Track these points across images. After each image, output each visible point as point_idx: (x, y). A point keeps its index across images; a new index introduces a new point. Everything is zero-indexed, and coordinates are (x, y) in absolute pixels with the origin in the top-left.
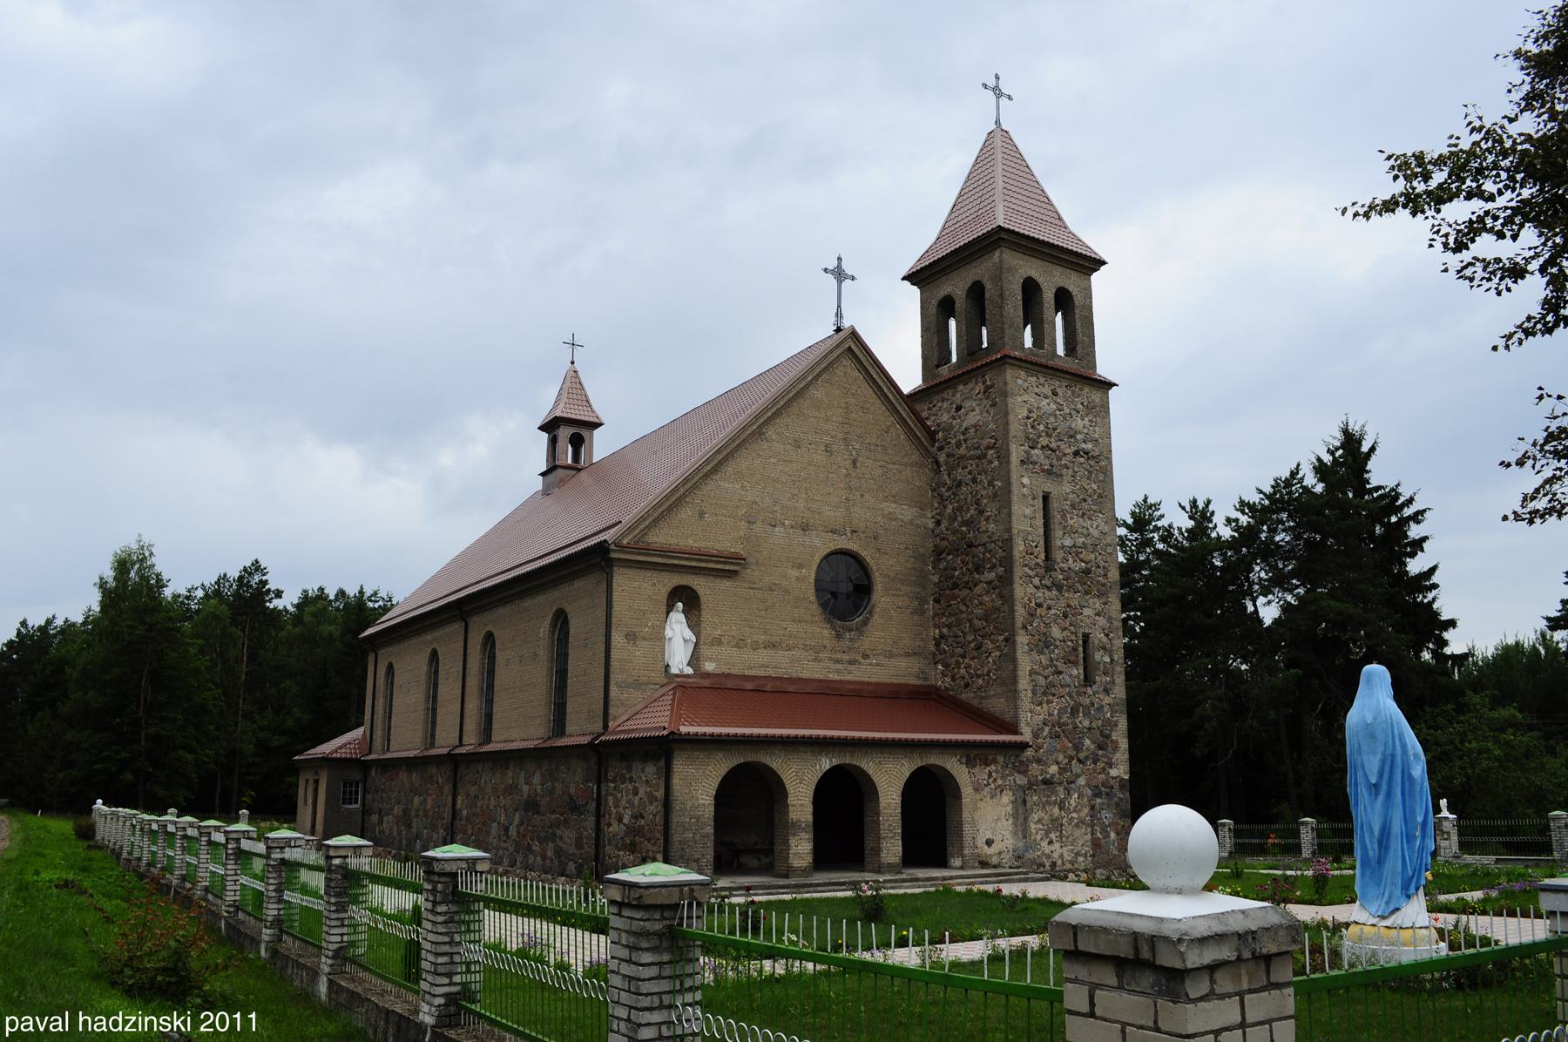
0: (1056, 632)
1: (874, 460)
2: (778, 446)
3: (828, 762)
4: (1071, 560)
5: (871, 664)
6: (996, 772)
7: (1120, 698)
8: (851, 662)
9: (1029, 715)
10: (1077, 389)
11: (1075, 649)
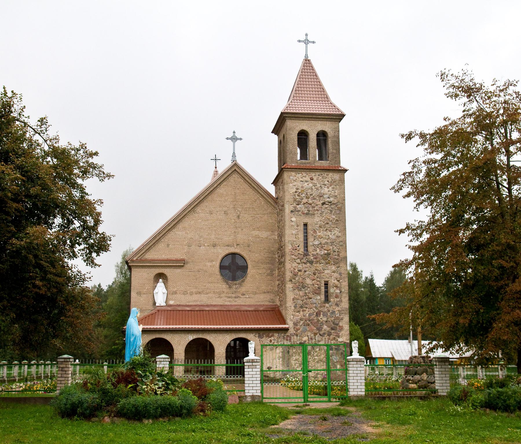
0: (308, 281)
1: (249, 214)
2: (202, 215)
3: (191, 337)
4: (318, 250)
5: (246, 298)
6: (274, 340)
7: (345, 308)
8: (235, 297)
9: (292, 316)
10: (325, 175)
11: (319, 288)
